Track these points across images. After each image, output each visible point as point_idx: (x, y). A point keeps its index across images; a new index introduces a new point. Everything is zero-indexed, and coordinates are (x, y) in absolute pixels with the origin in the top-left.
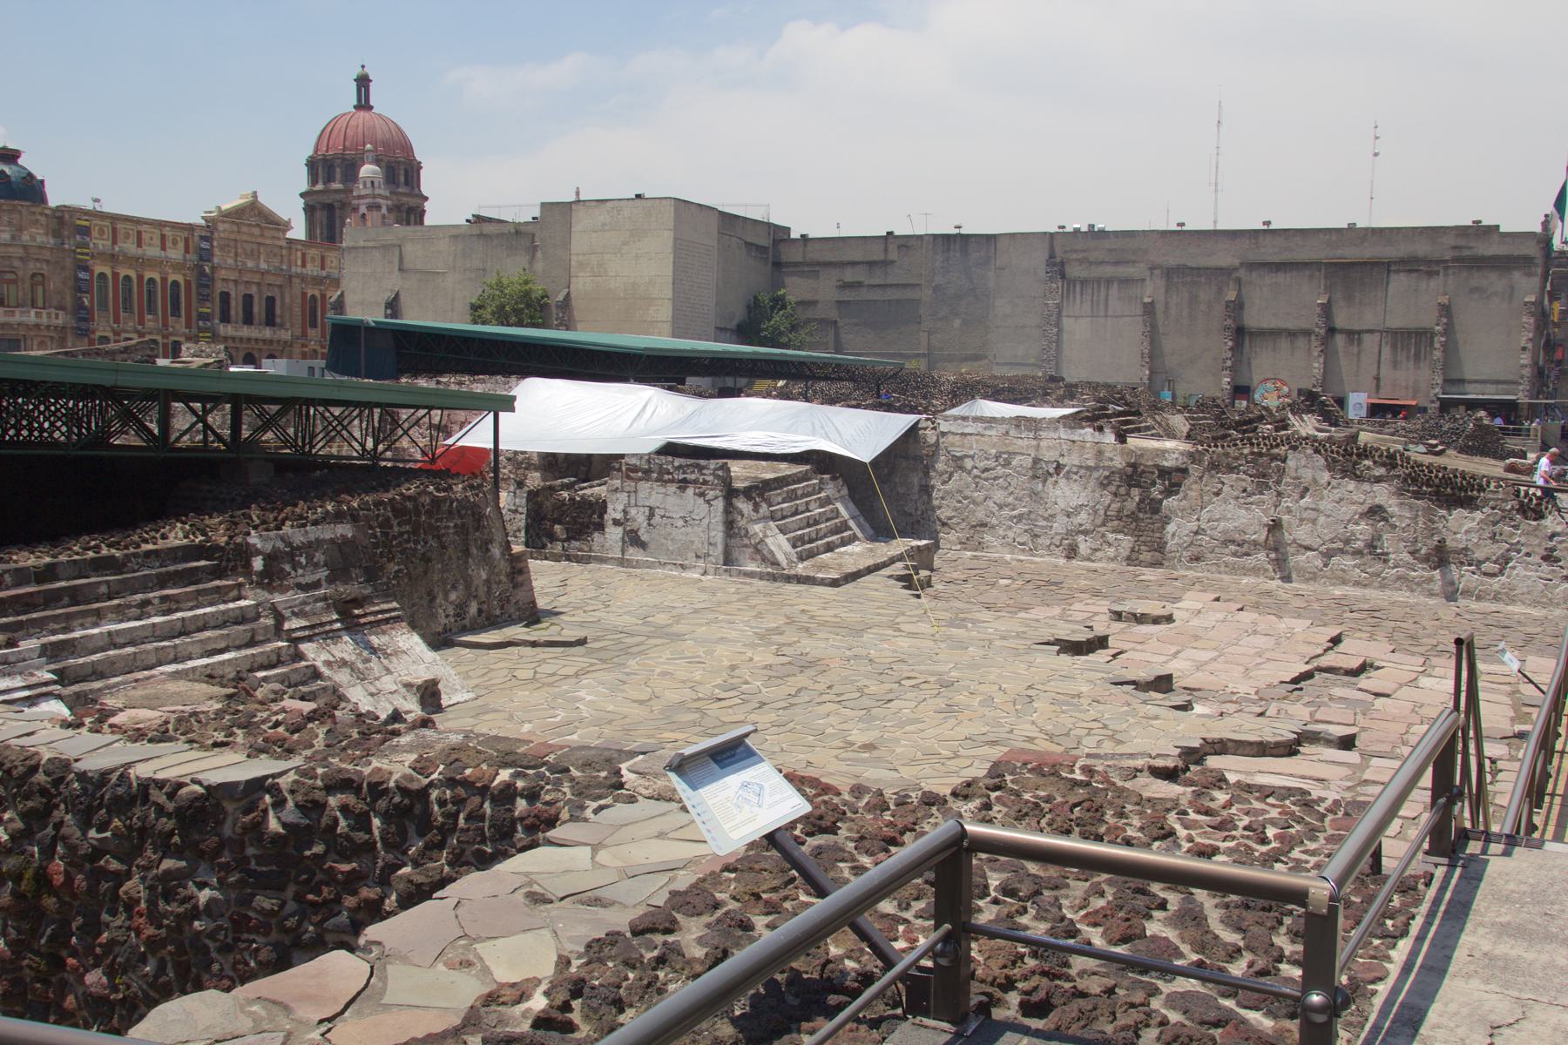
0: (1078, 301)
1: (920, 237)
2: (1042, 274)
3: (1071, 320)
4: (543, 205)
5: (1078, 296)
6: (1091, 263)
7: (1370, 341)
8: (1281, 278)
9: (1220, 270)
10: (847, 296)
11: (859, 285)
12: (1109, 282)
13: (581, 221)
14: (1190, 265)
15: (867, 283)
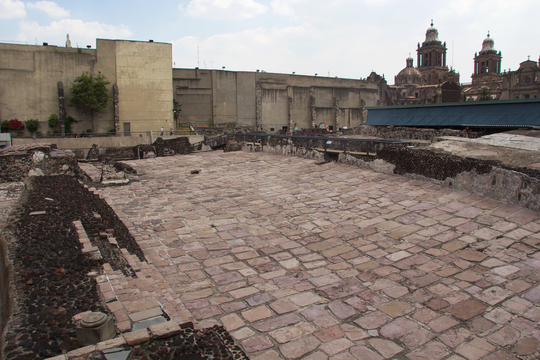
0: (267, 97)
1: (211, 71)
2: (254, 86)
3: (265, 103)
4: (98, 40)
5: (267, 95)
6: (269, 83)
7: (347, 111)
8: (323, 92)
9: (306, 88)
10: (182, 92)
11: (186, 88)
12: (276, 90)
13: (121, 51)
14: (298, 86)
15: (189, 87)
